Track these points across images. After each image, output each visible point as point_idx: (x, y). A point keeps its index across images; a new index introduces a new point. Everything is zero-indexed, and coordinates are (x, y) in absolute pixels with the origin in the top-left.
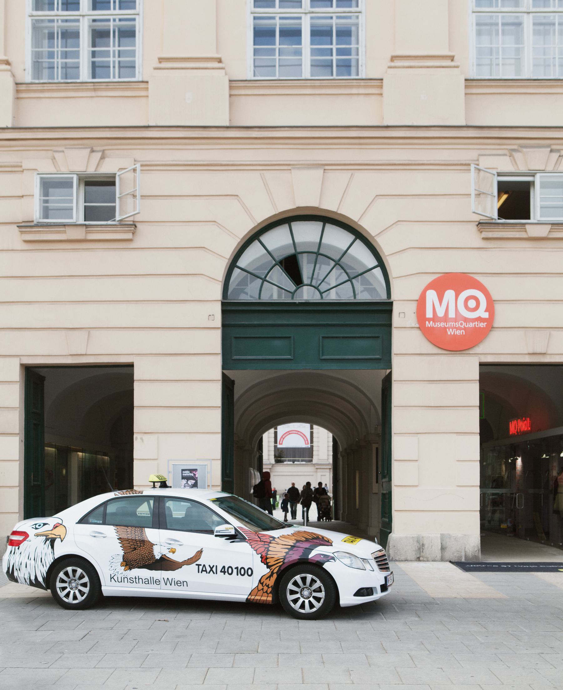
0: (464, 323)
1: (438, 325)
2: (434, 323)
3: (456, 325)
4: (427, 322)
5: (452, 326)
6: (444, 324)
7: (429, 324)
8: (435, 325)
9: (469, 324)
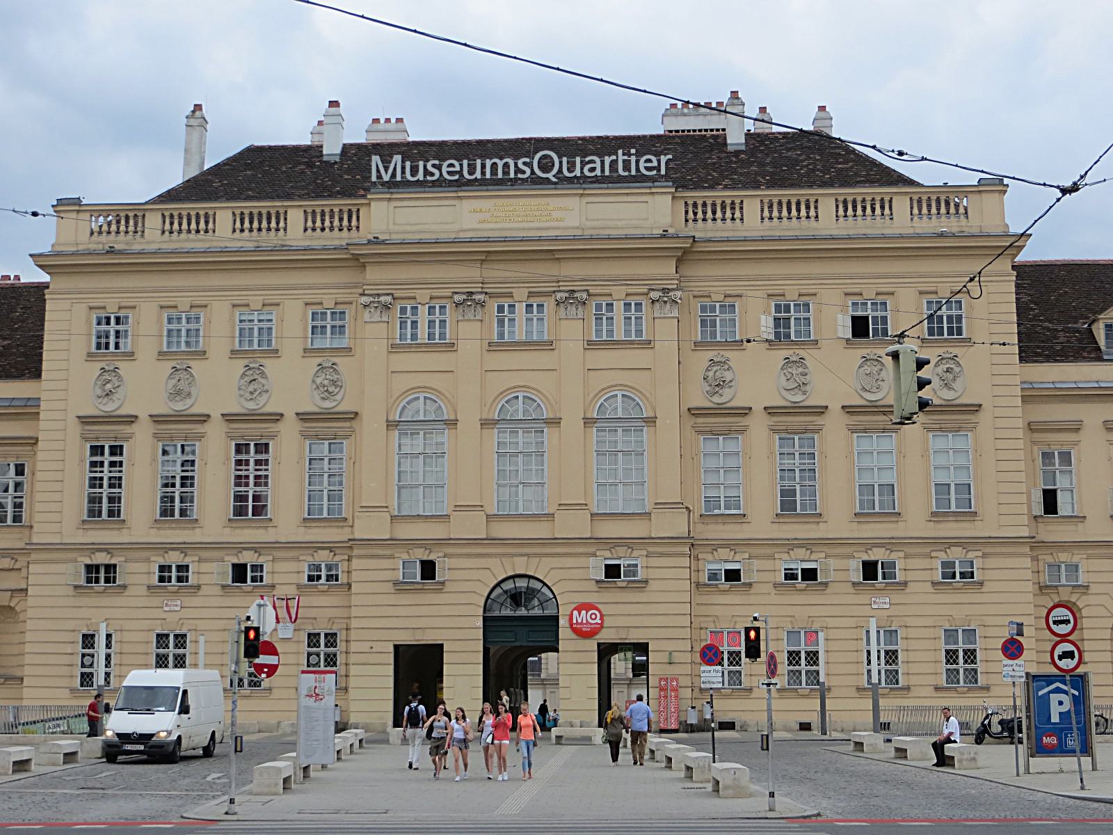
0: (560, 157)
1: (432, 174)
2: (408, 164)
3: (518, 170)
4: (376, 159)
5: (500, 175)
6: (457, 168)
7: (386, 172)
8: (414, 171)
9: (583, 164)
